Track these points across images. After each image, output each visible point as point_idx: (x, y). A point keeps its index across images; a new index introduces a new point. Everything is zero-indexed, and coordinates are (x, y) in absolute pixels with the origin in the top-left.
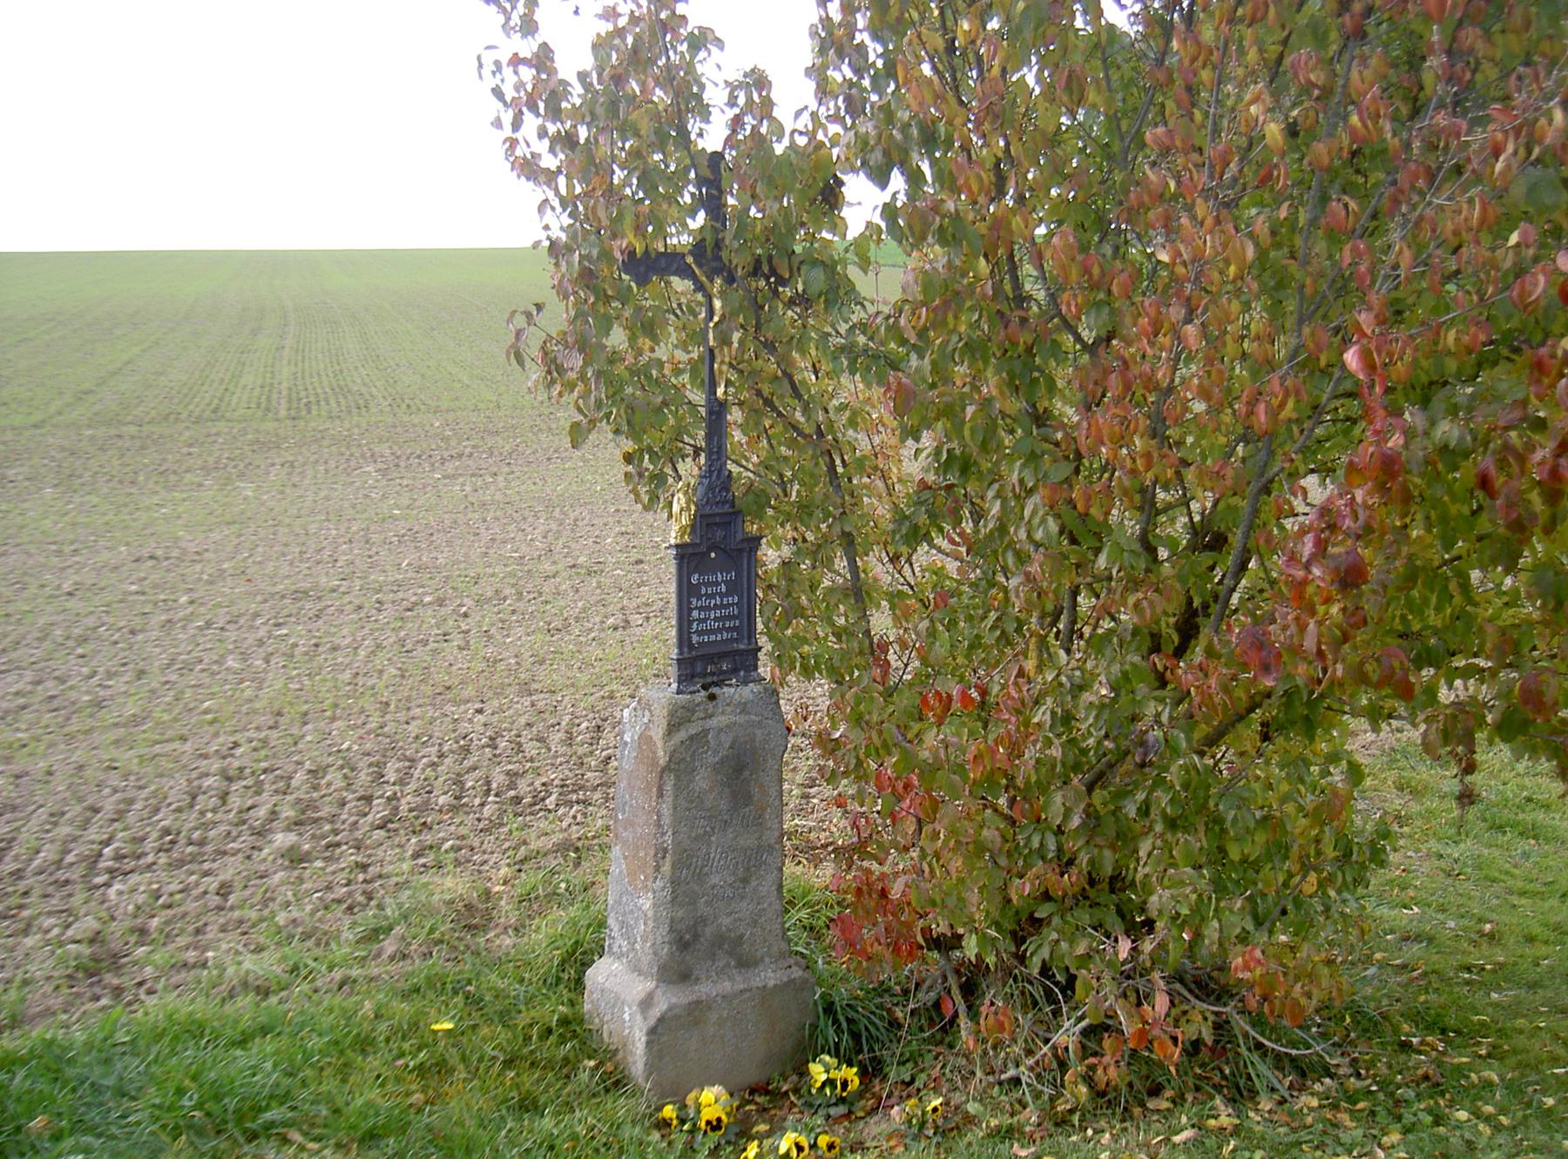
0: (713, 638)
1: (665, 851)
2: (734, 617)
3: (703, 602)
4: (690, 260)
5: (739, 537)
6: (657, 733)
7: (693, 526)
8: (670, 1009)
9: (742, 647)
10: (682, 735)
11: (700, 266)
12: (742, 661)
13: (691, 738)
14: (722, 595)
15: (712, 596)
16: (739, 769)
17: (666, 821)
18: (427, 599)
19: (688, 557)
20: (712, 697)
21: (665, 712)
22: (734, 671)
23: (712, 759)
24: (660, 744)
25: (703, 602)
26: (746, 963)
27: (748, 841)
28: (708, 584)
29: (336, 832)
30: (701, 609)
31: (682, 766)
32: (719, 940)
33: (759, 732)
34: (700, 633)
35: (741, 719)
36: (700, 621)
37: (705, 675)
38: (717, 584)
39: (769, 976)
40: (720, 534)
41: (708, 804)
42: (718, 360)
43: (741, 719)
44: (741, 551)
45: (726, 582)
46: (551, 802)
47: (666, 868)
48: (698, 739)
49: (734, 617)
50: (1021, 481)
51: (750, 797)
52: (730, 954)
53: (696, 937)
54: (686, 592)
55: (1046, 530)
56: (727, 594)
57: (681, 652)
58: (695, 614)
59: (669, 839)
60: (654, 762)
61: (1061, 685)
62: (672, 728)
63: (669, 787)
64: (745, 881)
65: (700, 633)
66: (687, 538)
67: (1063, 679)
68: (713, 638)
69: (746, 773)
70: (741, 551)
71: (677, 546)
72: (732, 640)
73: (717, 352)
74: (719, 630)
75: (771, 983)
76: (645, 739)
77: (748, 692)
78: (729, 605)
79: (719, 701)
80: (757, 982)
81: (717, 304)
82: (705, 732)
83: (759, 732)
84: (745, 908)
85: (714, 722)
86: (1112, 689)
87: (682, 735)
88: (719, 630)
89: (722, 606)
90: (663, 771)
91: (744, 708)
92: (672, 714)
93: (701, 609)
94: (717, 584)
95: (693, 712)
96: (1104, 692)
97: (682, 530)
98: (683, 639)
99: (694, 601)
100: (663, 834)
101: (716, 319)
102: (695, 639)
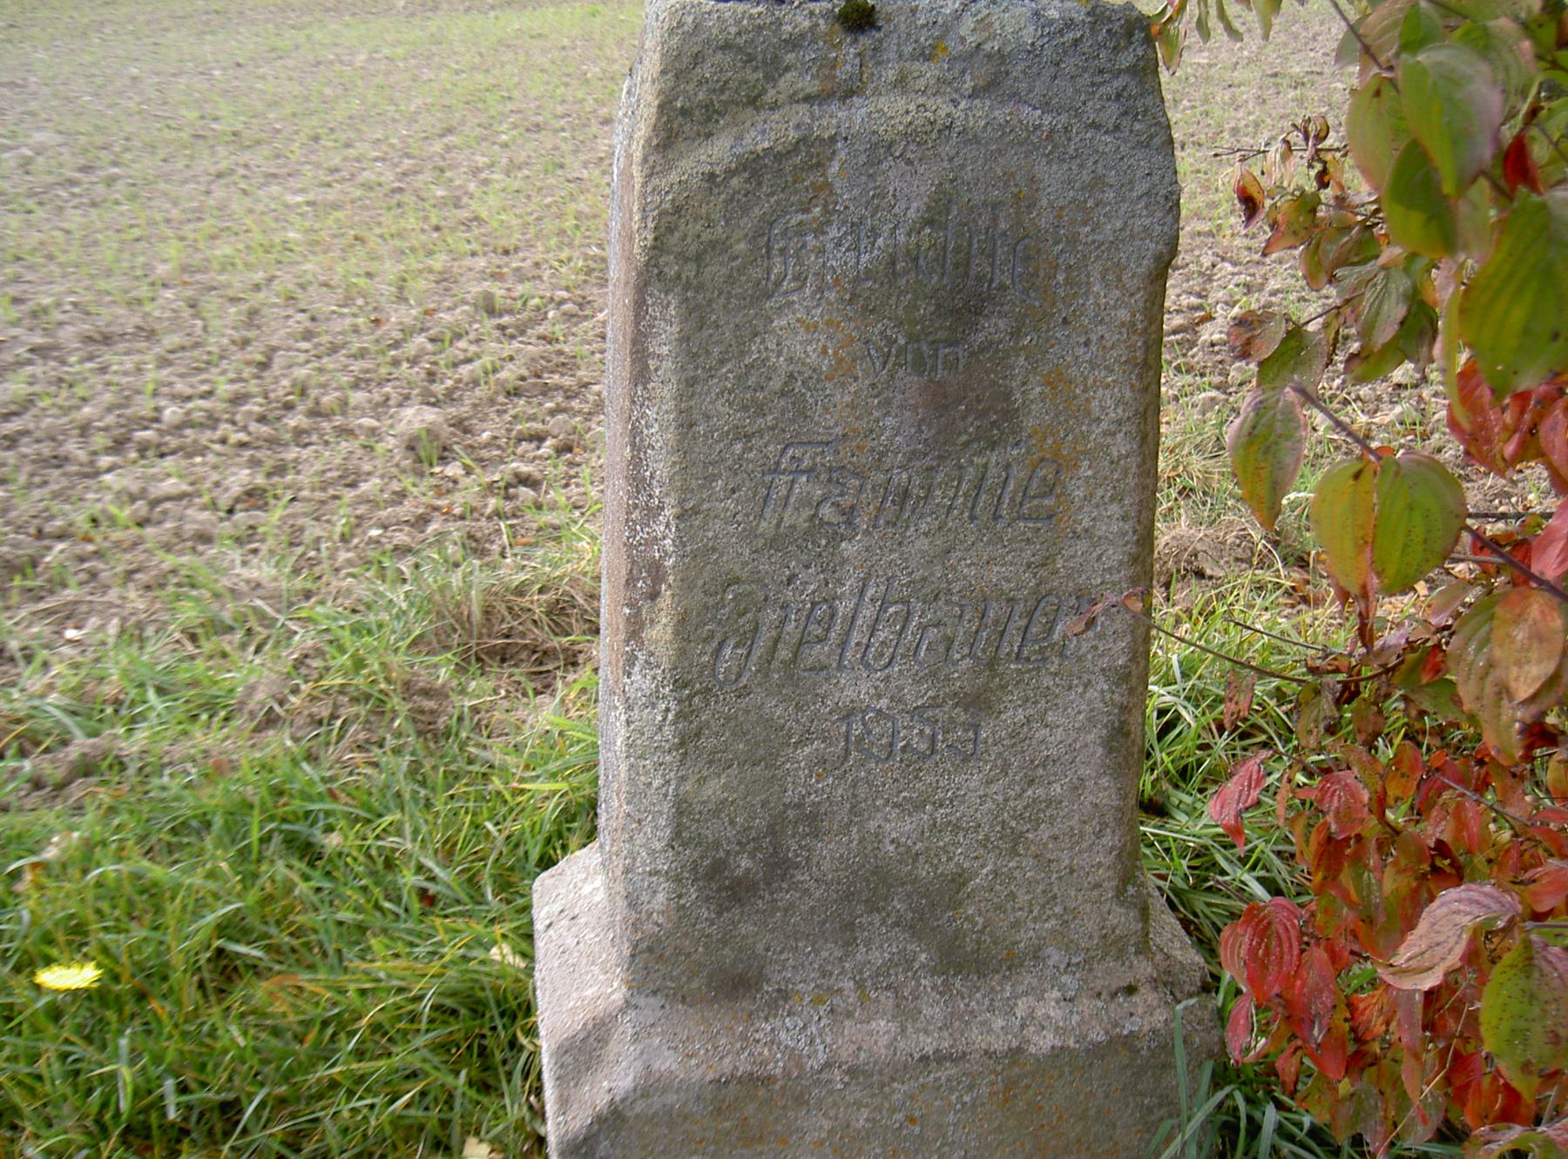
1: (656, 572)
8: (643, 1091)
10: (719, 151)
13: (752, 166)
16: (965, 305)
17: (660, 467)
26: (969, 961)
27: (1001, 569)
31: (715, 270)
32: (871, 886)
33: (1051, 176)
35: (978, 114)
39: (1045, 1016)
41: (828, 422)
43: (978, 114)
47: (660, 631)
51: (1010, 414)
52: (917, 928)
53: (779, 867)
59: (665, 530)
62: (678, 123)
63: (664, 345)
64: (978, 703)
69: (994, 326)
75: (1044, 1042)
80: (992, 1032)
82: (811, 152)
83: (1051, 176)
84: (975, 792)
85: (855, 116)
87: (719, 151)
95: (774, 68)
100: (652, 513)
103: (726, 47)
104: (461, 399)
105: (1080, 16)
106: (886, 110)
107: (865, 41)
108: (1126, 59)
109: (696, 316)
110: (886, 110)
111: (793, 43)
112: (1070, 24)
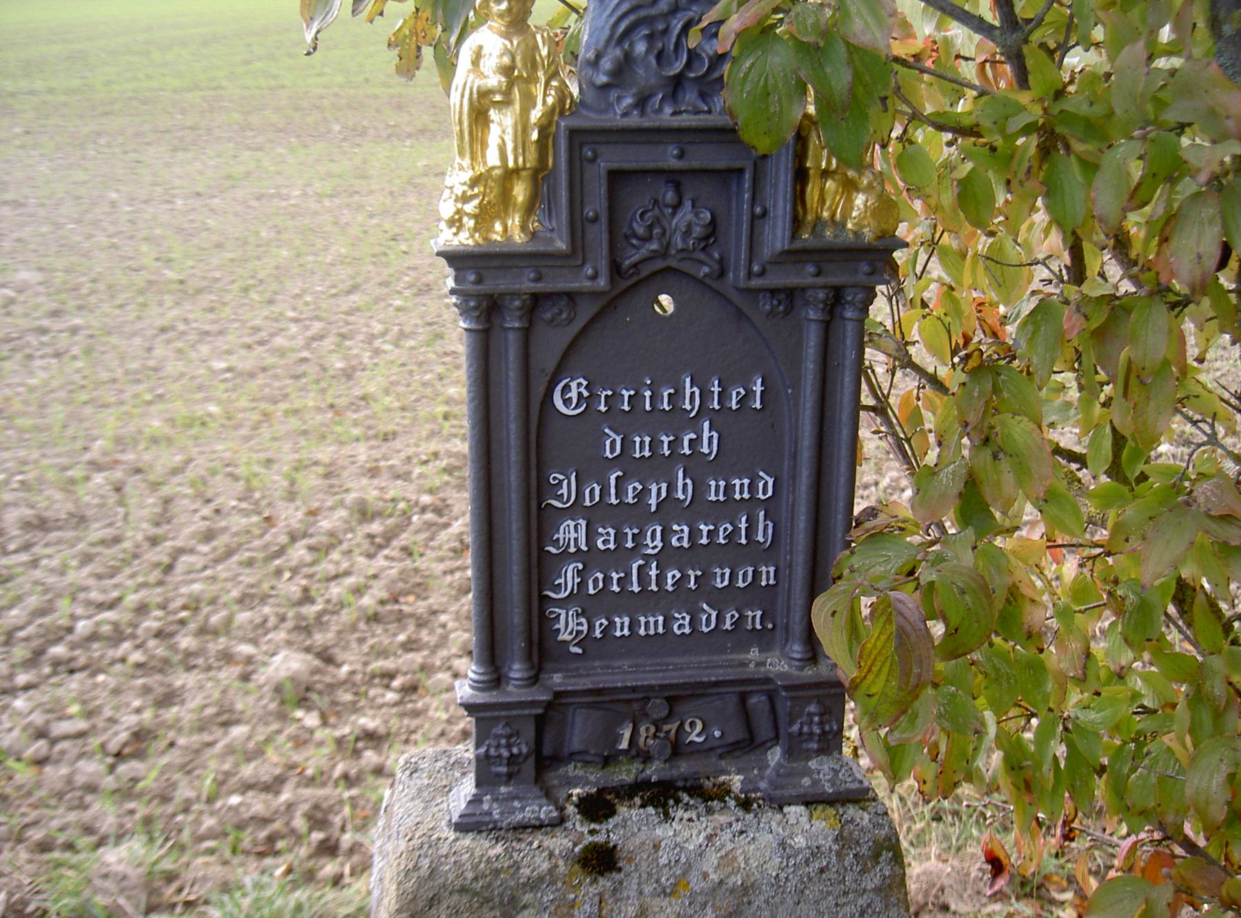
0: (652, 624)
2: (754, 553)
7: (540, 177)
14: (696, 465)
15: (657, 467)
20: (600, 860)
28: (630, 421)
29: (409, 646)
30: (595, 516)
36: (590, 558)
38: (677, 420)
45: (720, 419)
54: (519, 459)
56: (724, 464)
57: (495, 677)
58: (571, 533)
66: (511, 230)
68: (652, 624)
72: (741, 636)
78: (728, 508)
79: (632, 882)
89: (697, 509)
94: (677, 420)
97: (494, 192)
98: (515, 622)
99: (566, 487)
102: (568, 625)
103: (463, 890)
104: (327, 622)
105: (827, 843)
107: (605, 883)
108: (872, 881)
111: (534, 885)
112: (816, 852)
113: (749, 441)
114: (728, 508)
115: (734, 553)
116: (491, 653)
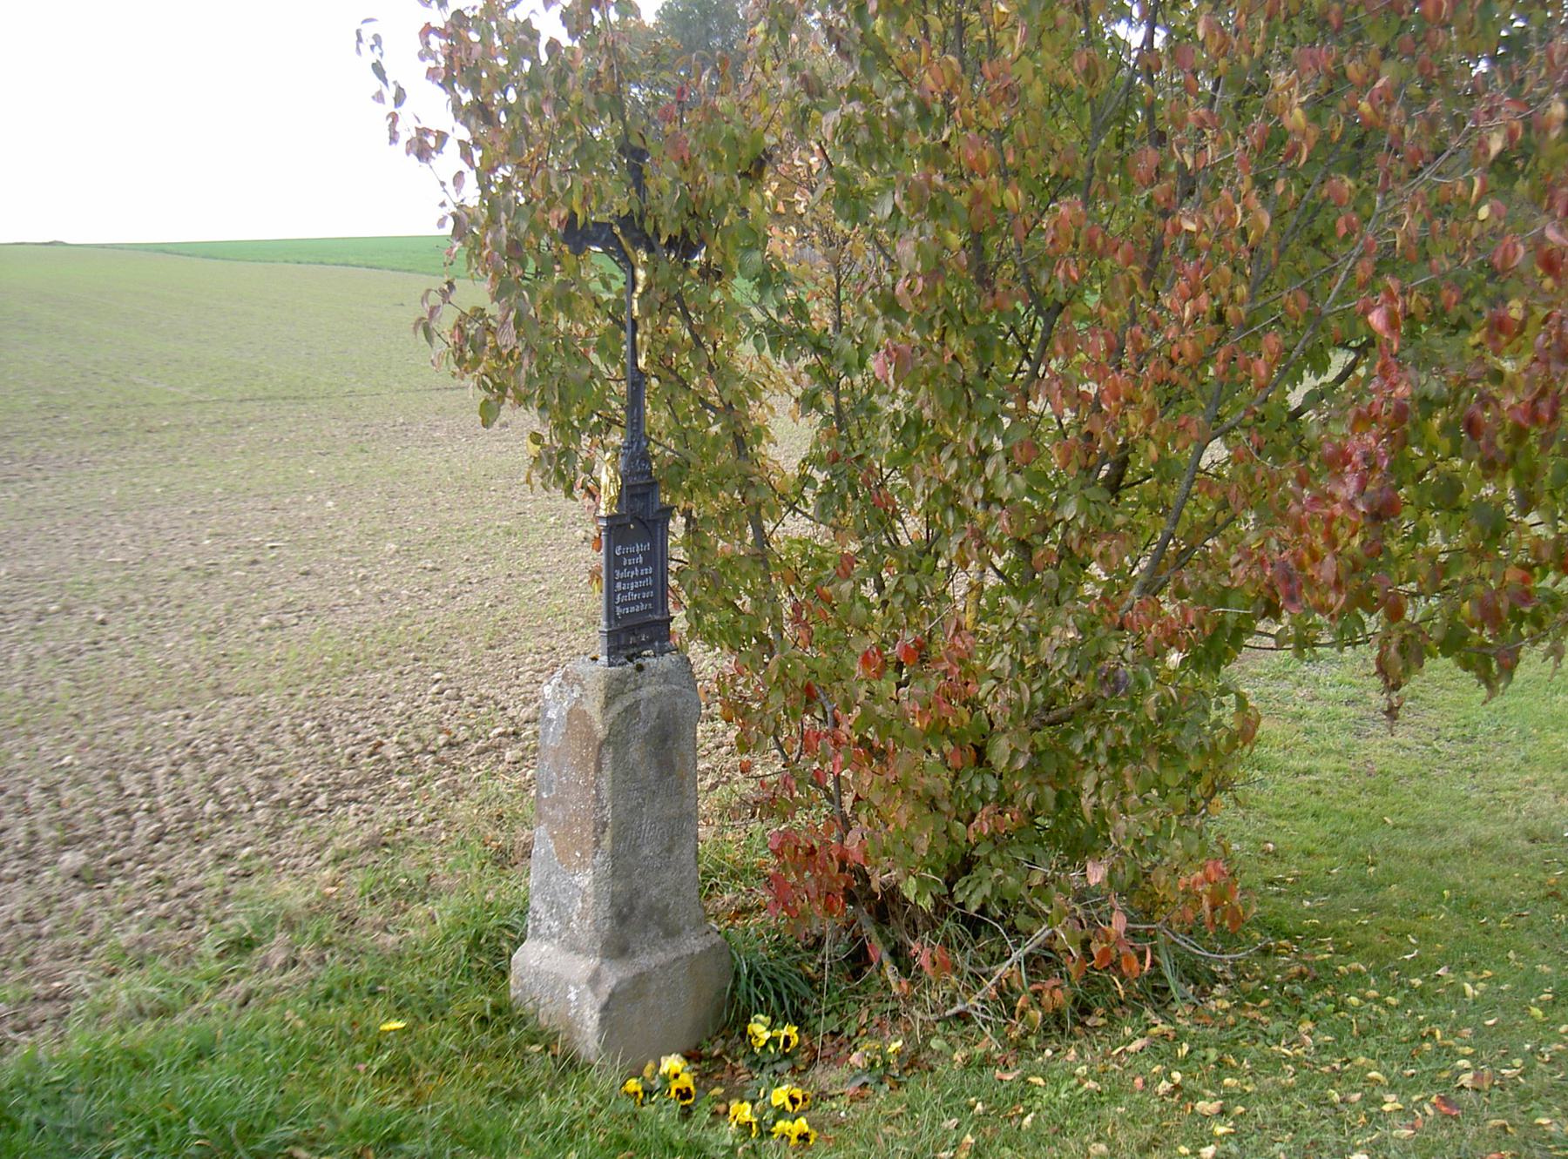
1: (605, 825)
3: (625, 574)
4: (617, 230)
5: (657, 507)
6: (593, 707)
7: (620, 498)
8: (619, 983)
9: (657, 617)
10: (618, 707)
11: (625, 236)
12: (658, 631)
13: (626, 710)
16: (664, 740)
17: (605, 794)
18: (54, 608)
19: (616, 530)
20: (640, 668)
21: (601, 685)
22: (650, 643)
23: (642, 730)
24: (597, 718)
25: (625, 574)
26: (671, 933)
27: (672, 811)
30: (624, 580)
32: (651, 909)
33: (679, 701)
34: (623, 605)
35: (664, 688)
36: (624, 592)
37: (627, 647)
38: (635, 555)
39: (693, 944)
40: (639, 505)
41: (640, 775)
42: (641, 330)
43: (664, 688)
44: (655, 522)
46: (321, 801)
47: (606, 842)
48: (631, 710)
49: (646, 588)
50: (977, 441)
52: (659, 924)
53: (632, 909)
55: (1013, 486)
57: (609, 626)
58: (619, 585)
59: (608, 812)
60: (590, 734)
61: (1019, 632)
62: (609, 701)
64: (670, 850)
65: (623, 605)
67: (1021, 626)
70: (655, 522)
71: (608, 518)
72: (648, 611)
73: (640, 322)
74: (636, 602)
75: (698, 950)
76: (576, 715)
77: (668, 661)
78: (643, 577)
79: (646, 672)
80: (685, 951)
81: (641, 274)
82: (637, 703)
83: (679, 701)
84: (669, 876)
86: (1080, 631)
87: (618, 707)
88: (636, 602)
90: (602, 744)
91: (666, 677)
92: (608, 687)
93: (624, 580)
94: (635, 555)
95: (626, 683)
96: (1071, 635)
97: (610, 503)
100: (603, 808)
101: (640, 289)
102: (619, 610)
106: (646, 692)
109: (616, 751)
110: (646, 692)
113: (649, 558)
114: (643, 577)
115: (646, 588)
116: (608, 619)
